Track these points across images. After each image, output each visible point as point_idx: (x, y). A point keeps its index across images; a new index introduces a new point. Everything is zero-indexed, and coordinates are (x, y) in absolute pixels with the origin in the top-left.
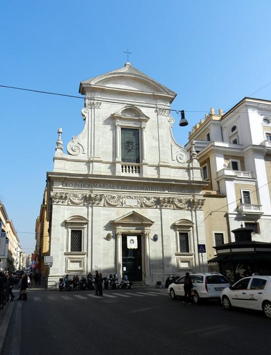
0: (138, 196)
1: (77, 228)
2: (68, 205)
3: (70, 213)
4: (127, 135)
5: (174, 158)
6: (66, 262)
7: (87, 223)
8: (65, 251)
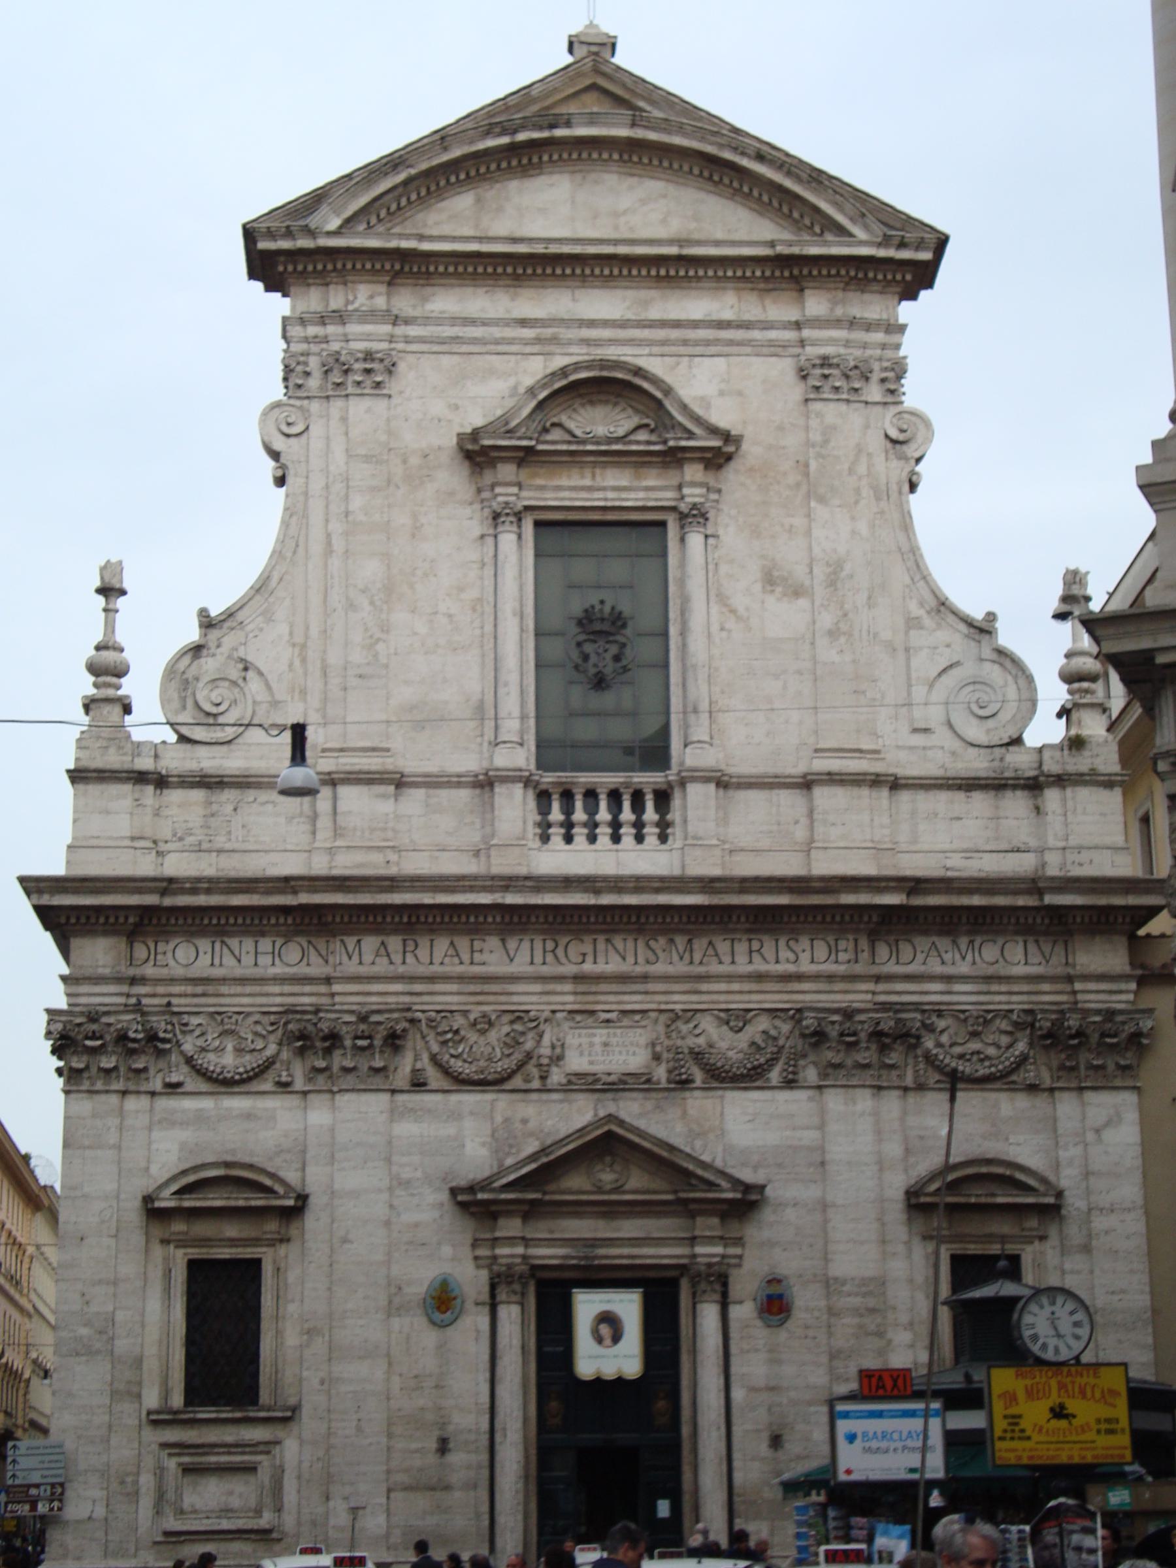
2: (173, 1088)
3: (183, 1146)
4: (583, 570)
5: (934, 716)
6: (160, 1472)
8: (151, 1400)
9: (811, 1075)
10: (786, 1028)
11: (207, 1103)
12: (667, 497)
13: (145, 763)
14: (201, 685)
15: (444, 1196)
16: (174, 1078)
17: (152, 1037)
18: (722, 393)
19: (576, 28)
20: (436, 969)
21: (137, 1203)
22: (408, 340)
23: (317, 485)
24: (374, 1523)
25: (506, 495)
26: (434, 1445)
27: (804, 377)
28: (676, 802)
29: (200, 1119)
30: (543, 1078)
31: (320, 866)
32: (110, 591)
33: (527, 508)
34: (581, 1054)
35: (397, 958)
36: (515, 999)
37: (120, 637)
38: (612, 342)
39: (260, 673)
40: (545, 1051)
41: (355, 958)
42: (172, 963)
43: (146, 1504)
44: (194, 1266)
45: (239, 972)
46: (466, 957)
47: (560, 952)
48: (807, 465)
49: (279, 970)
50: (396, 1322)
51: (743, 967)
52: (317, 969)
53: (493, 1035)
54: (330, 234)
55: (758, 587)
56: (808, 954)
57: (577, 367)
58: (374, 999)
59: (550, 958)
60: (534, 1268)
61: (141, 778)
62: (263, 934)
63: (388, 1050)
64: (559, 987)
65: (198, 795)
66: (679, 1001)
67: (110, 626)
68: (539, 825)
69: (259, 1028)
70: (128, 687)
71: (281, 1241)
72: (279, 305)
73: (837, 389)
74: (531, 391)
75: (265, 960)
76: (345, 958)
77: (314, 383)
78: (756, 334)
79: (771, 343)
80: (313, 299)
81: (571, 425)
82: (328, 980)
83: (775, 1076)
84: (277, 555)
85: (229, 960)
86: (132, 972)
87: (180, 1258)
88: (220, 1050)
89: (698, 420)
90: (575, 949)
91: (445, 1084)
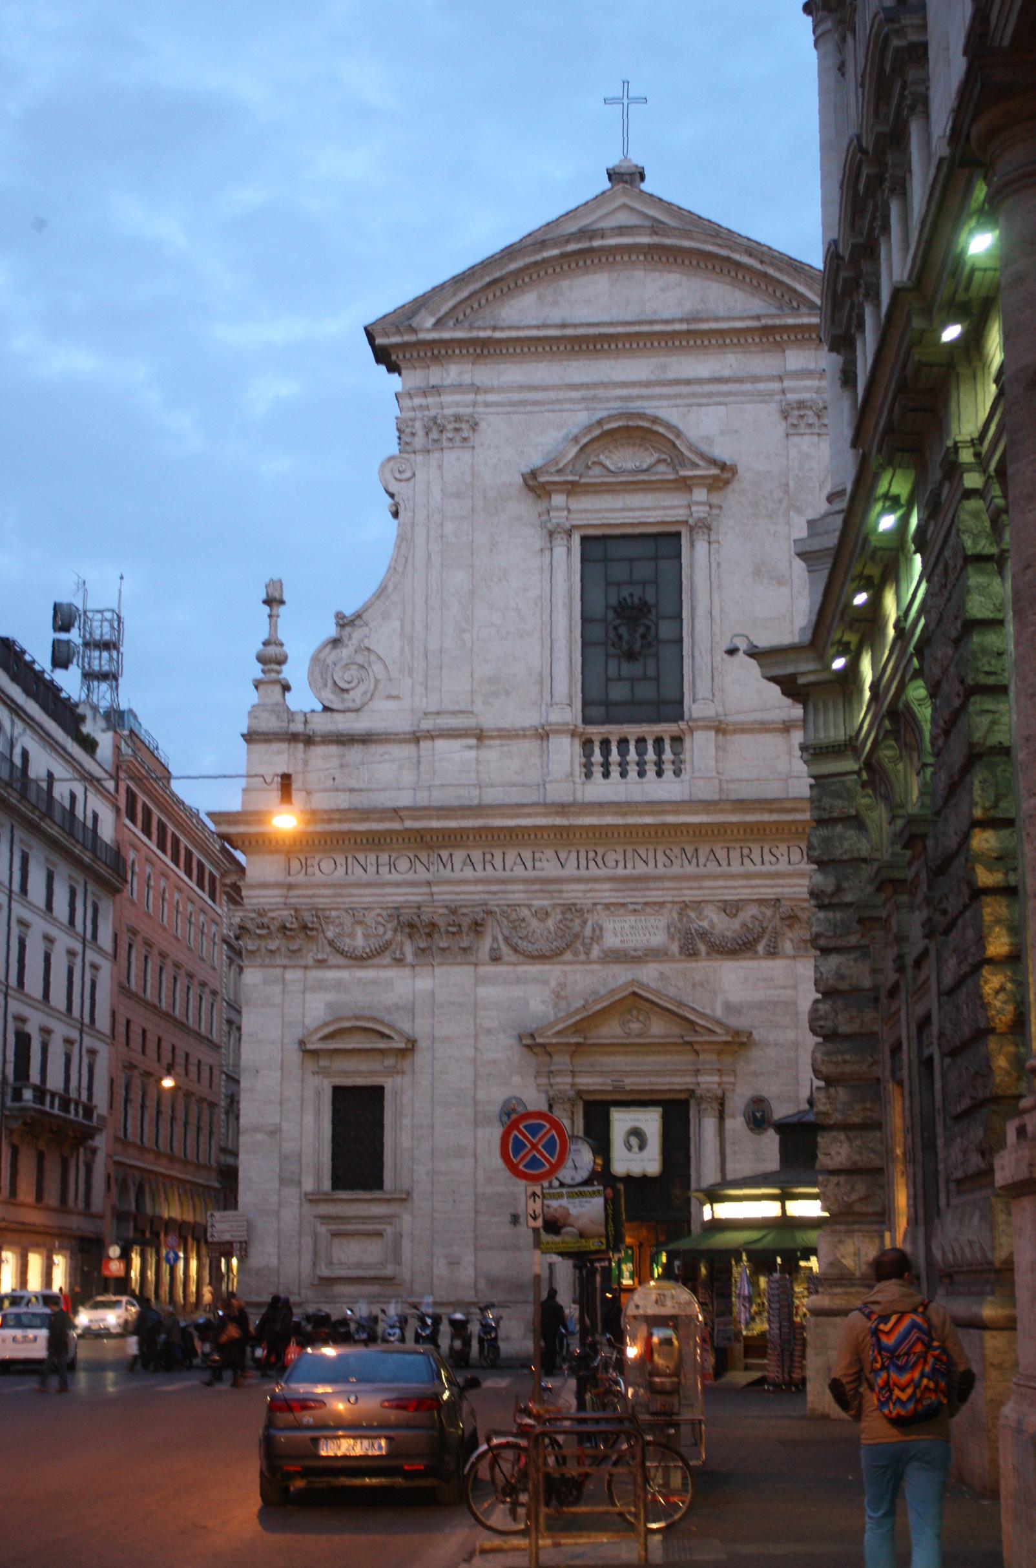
1: (359, 1074)
2: (321, 963)
3: (329, 1005)
6: (315, 1235)
8: (308, 1185)
9: (788, 947)
10: (769, 913)
11: (344, 974)
12: (680, 514)
13: (298, 727)
14: (337, 668)
15: (513, 1042)
16: (320, 957)
17: (305, 927)
18: (722, 432)
19: (611, 166)
20: (508, 874)
21: (296, 1046)
22: (487, 405)
23: (421, 516)
24: (466, 1274)
25: (559, 517)
26: (508, 1218)
27: (786, 418)
28: (687, 744)
29: (339, 986)
30: (587, 954)
31: (422, 798)
32: (274, 602)
33: (574, 527)
34: (616, 935)
35: (479, 867)
36: (565, 895)
37: (282, 636)
38: (640, 397)
39: (380, 658)
40: (588, 932)
41: (449, 867)
42: (318, 872)
43: (307, 1257)
44: (338, 1091)
45: (365, 877)
46: (529, 864)
47: (599, 860)
48: (787, 485)
49: (395, 877)
50: (481, 1132)
51: (736, 868)
52: (422, 874)
53: (550, 923)
54: (428, 330)
56: (786, 858)
57: (611, 418)
58: (462, 897)
59: (592, 864)
60: (580, 1093)
61: (293, 738)
62: (382, 850)
63: (472, 934)
64: (597, 886)
65: (333, 749)
66: (689, 895)
67: (273, 627)
68: (585, 766)
69: (380, 919)
70: (288, 672)
71: (398, 1073)
72: (395, 382)
73: (810, 425)
74: (576, 439)
75: (384, 870)
76: (441, 866)
77: (419, 441)
78: (748, 387)
79: (760, 393)
80: (415, 377)
81: (608, 463)
82: (429, 884)
83: (760, 948)
84: (392, 570)
85: (359, 871)
86: (291, 880)
87: (326, 1087)
88: (352, 936)
89: (702, 455)
90: (611, 858)
91: (513, 958)
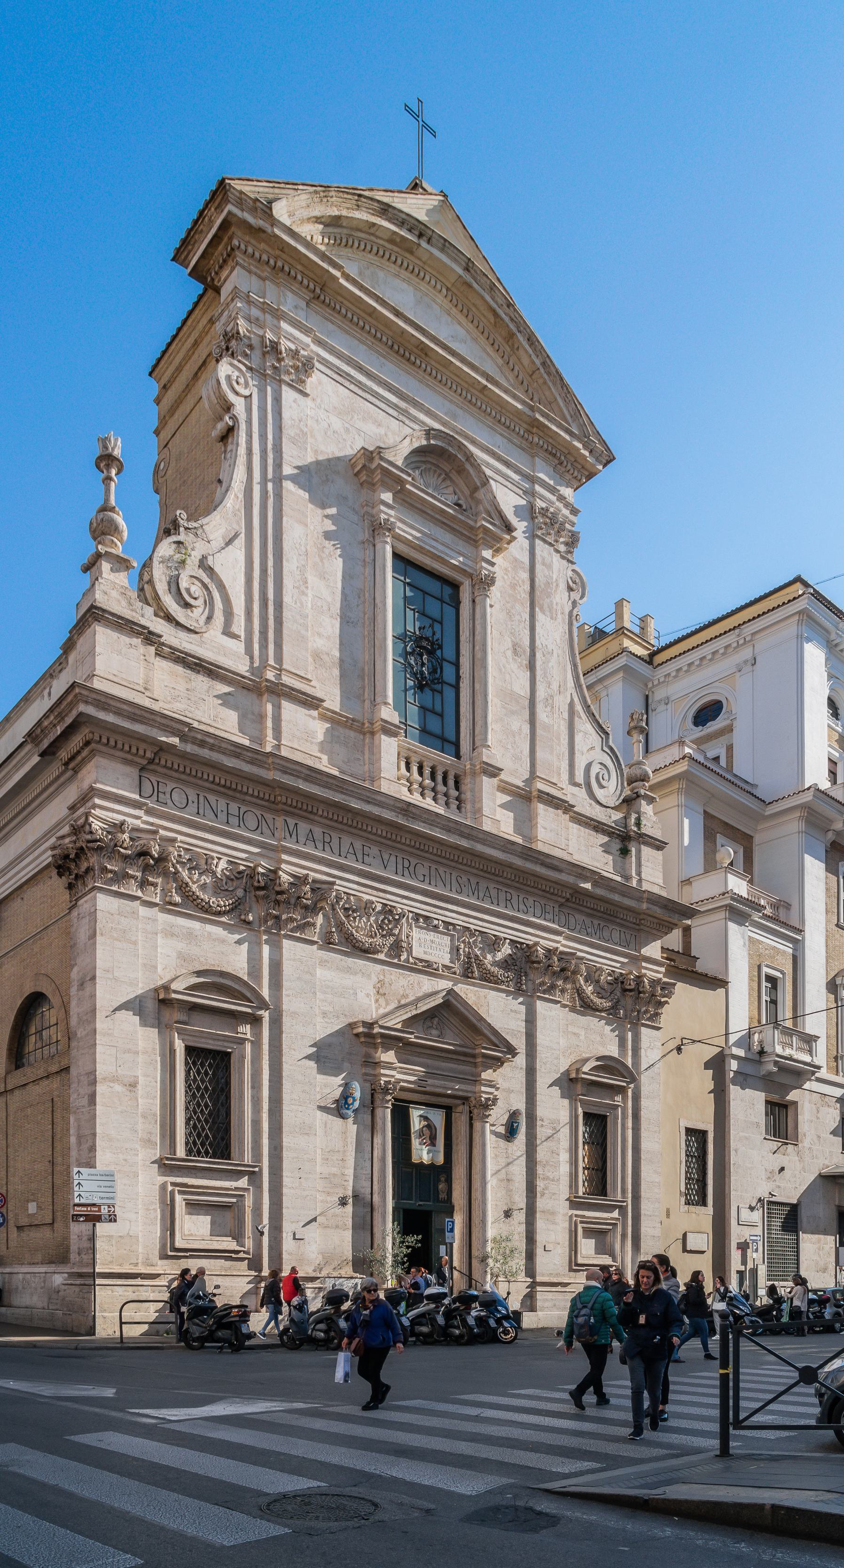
0: (460, 921)
7: (255, 1021)
10: (519, 954)
42: (169, 801)
47: (412, 869)
55: (509, 653)
